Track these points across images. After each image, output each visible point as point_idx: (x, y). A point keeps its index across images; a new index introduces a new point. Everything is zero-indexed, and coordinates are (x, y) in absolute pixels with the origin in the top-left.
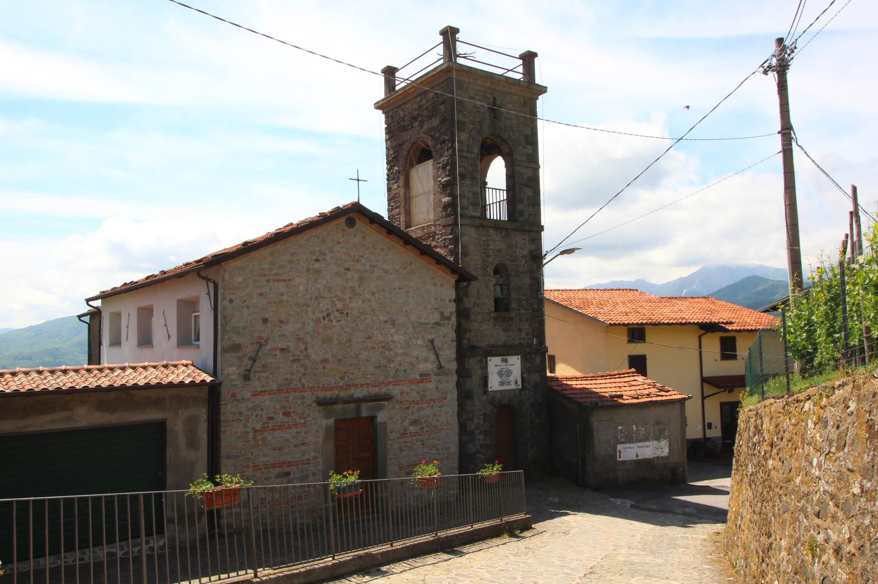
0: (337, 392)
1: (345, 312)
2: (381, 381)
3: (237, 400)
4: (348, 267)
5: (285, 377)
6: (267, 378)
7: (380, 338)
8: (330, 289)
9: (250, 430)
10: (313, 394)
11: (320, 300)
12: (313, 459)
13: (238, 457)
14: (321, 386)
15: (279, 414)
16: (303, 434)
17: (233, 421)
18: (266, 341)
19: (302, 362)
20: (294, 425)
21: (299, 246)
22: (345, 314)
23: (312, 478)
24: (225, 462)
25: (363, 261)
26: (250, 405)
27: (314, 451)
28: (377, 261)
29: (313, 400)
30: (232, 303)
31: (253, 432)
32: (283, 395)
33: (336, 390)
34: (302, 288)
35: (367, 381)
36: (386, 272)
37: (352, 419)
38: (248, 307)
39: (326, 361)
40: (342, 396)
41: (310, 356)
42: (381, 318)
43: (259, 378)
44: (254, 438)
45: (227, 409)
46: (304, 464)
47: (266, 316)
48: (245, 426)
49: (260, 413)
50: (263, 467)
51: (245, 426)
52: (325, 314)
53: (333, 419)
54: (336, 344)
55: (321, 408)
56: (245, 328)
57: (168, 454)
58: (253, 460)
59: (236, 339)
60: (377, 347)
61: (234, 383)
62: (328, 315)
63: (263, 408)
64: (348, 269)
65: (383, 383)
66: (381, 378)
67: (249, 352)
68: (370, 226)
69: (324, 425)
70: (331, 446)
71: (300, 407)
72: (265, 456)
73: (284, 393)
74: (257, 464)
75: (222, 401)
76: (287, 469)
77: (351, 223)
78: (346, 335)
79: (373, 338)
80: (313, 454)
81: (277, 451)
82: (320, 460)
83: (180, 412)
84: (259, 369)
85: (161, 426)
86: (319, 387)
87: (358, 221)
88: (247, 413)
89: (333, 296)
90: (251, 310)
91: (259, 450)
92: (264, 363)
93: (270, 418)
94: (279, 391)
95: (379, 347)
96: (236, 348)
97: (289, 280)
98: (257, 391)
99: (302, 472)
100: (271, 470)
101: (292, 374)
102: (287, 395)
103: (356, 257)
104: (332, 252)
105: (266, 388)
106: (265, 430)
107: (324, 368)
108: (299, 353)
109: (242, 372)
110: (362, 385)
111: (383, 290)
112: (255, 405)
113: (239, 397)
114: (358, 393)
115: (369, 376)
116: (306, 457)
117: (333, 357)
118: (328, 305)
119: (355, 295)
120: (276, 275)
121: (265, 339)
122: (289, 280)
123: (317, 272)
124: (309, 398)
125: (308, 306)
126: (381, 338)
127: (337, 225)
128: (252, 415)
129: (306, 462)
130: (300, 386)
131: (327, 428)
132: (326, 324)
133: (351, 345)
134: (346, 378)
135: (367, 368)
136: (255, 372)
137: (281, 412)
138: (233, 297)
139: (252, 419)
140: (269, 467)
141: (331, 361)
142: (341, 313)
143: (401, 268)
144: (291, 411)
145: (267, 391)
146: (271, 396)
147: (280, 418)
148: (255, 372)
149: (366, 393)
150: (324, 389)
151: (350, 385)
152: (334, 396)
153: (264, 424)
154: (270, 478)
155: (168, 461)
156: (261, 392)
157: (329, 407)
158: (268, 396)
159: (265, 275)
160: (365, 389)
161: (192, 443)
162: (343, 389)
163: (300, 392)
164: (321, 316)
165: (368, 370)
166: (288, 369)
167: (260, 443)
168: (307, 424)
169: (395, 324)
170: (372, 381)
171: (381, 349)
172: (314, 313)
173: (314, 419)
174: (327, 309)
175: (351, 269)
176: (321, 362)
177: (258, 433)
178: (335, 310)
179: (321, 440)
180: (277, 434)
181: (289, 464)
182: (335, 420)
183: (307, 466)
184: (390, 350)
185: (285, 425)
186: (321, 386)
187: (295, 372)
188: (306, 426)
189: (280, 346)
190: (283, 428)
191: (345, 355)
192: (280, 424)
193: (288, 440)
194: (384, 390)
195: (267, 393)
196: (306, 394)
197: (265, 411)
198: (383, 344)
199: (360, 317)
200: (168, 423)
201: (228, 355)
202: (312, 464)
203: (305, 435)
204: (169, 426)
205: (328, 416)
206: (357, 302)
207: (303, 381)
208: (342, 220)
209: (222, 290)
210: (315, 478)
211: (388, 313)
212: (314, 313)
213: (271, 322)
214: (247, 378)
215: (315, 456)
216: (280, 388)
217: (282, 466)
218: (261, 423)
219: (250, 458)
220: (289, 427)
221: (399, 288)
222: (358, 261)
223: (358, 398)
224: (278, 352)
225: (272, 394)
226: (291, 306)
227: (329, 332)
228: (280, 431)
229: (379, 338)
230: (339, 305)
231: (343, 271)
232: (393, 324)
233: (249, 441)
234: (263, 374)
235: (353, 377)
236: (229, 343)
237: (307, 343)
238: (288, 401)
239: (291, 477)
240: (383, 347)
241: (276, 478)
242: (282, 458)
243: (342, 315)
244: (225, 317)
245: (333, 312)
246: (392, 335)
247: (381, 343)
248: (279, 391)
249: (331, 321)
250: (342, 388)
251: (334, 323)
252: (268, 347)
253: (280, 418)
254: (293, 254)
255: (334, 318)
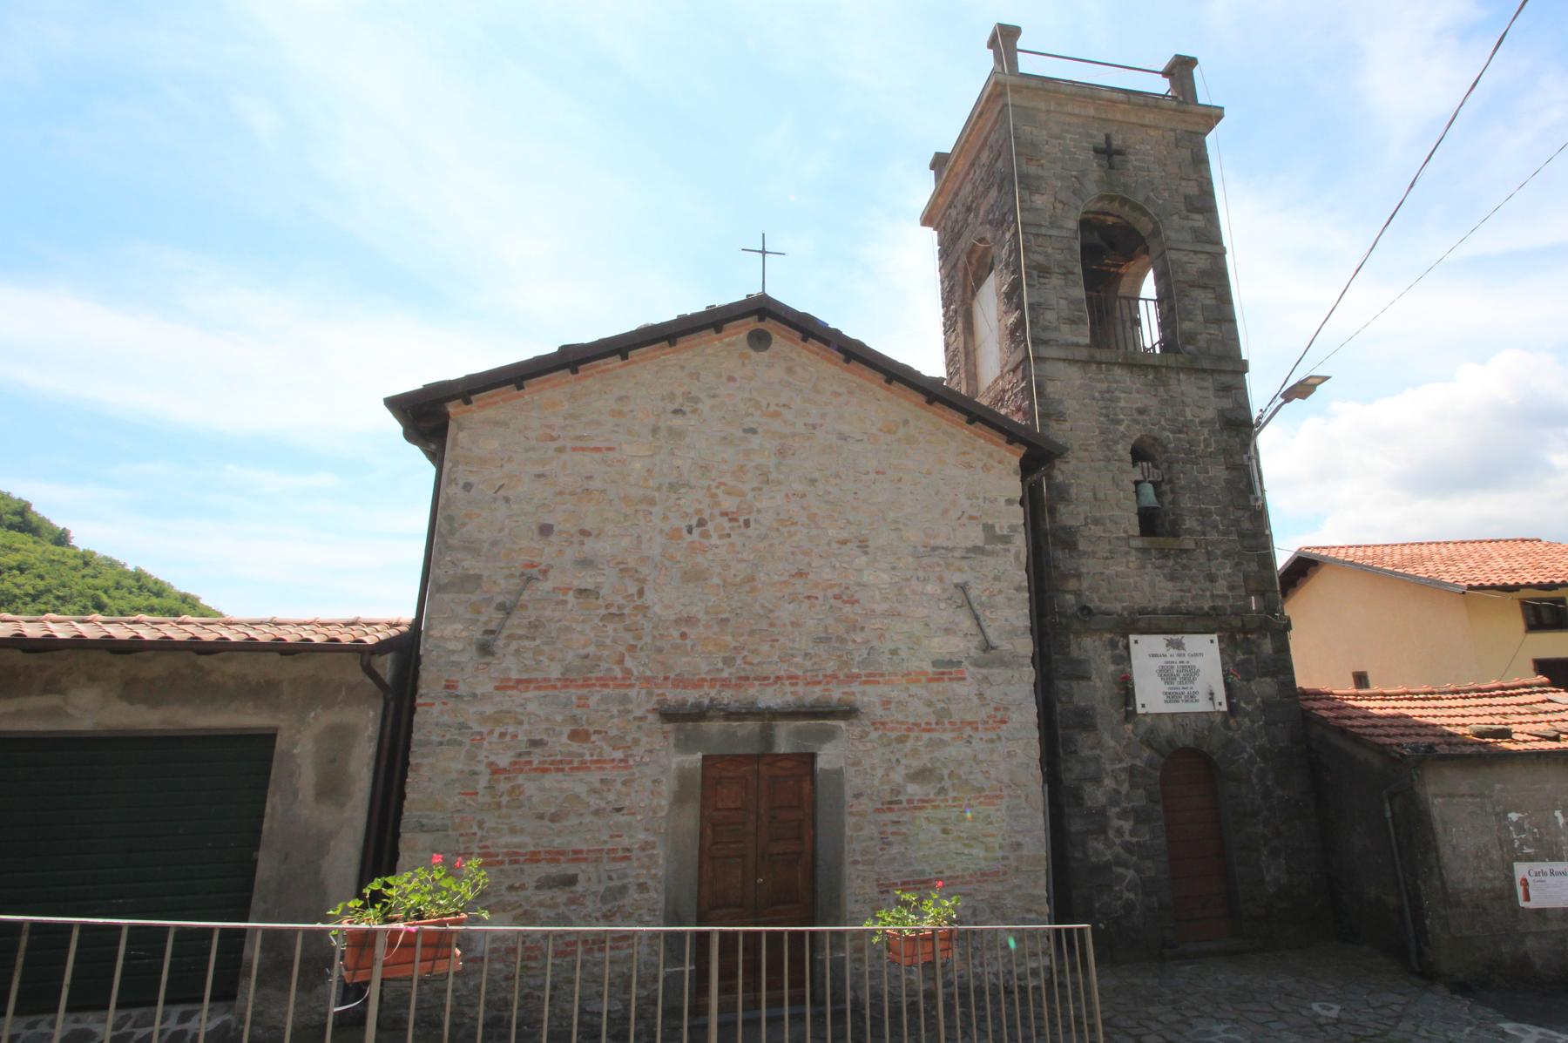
0: (713, 693)
1: (742, 519)
2: (829, 672)
3: (457, 696)
4: (752, 426)
5: (583, 652)
6: (537, 652)
7: (827, 574)
8: (705, 468)
9: (481, 768)
10: (650, 694)
11: (682, 491)
12: (643, 849)
13: (444, 829)
14: (672, 675)
15: (561, 733)
16: (619, 786)
17: (441, 744)
18: (545, 572)
19: (628, 622)
20: (598, 761)
21: (637, 383)
22: (741, 523)
23: (636, 896)
24: (409, 840)
25: (788, 415)
26: (489, 710)
27: (647, 830)
28: (823, 415)
29: (650, 706)
30: (469, 491)
31: (489, 771)
32: (573, 691)
33: (712, 686)
34: (637, 465)
35: (792, 669)
36: (844, 438)
37: (756, 758)
38: (507, 500)
39: (690, 621)
40: (726, 701)
41: (648, 608)
42: (831, 532)
43: (517, 652)
44: (490, 787)
45: (430, 717)
46: (614, 860)
47: (548, 520)
48: (472, 757)
49: (511, 729)
50: (507, 859)
51: (472, 757)
52: (694, 522)
53: (699, 755)
54: (718, 585)
55: (669, 727)
56: (494, 543)
57: (268, 810)
58: (481, 841)
59: (471, 564)
60: (820, 594)
61: (454, 658)
62: (701, 523)
63: (521, 717)
64: (753, 431)
65: (835, 677)
66: (831, 667)
67: (499, 593)
68: (804, 348)
69: (674, 766)
70: (690, 819)
71: (616, 720)
72: (513, 831)
73: (577, 687)
74: (491, 850)
75: (421, 696)
76: (570, 869)
77: (759, 340)
78: (743, 565)
79: (811, 576)
80: (642, 836)
81: (547, 823)
82: (659, 851)
83: (312, 714)
84: (520, 632)
85: (261, 744)
86: (666, 678)
87: (776, 338)
88: (476, 728)
89: (714, 484)
90: (514, 507)
91: (499, 817)
92: (532, 619)
93: (535, 743)
94: (566, 681)
95: (825, 596)
96: (469, 582)
97: (609, 449)
98: (509, 680)
99: (610, 878)
100: (527, 867)
101: (601, 645)
102: (585, 691)
103: (772, 408)
104: (714, 396)
105: (534, 675)
106: (521, 771)
107: (683, 636)
108: (622, 601)
109: (478, 634)
110: (778, 678)
111: (837, 476)
112: (502, 711)
113: (463, 689)
114: (770, 698)
115: (798, 660)
116: (626, 841)
117: (707, 613)
118: (700, 503)
119: (767, 482)
120: (578, 438)
121: (543, 567)
122: (609, 449)
123: (676, 434)
124: (641, 701)
125: (652, 502)
126: (830, 577)
127: (729, 344)
128: (491, 732)
129: (620, 854)
130: (618, 673)
131: (683, 777)
132: (693, 542)
133: (753, 590)
134: (739, 661)
135: (794, 641)
136: (511, 637)
137: (567, 730)
138: (472, 479)
139: (490, 743)
140: (522, 858)
141: (703, 622)
142: (731, 520)
143: (881, 430)
144: (591, 730)
145: (536, 680)
146: (542, 693)
147: (561, 743)
148: (511, 637)
149: (790, 698)
150: (680, 682)
151: (747, 678)
152: (706, 701)
153: (520, 755)
154: (523, 887)
155: (266, 826)
156: (519, 681)
157: (690, 725)
158: (537, 693)
159: (553, 439)
160: (788, 689)
161: (331, 788)
162: (727, 686)
163: (618, 686)
164: (683, 525)
165: (796, 645)
166: (592, 635)
167: (505, 799)
168: (631, 762)
169: (867, 546)
170: (806, 671)
171: (833, 602)
172: (665, 518)
173: (651, 751)
174: (699, 511)
175: (760, 430)
176: (677, 622)
177: (502, 777)
178: (716, 512)
179: (664, 803)
180: (549, 780)
181: (577, 856)
182: (704, 757)
183: (624, 865)
184: (853, 602)
185: (570, 762)
186: (672, 675)
187: (608, 642)
188: (626, 768)
189: (577, 583)
190: (567, 767)
191: (739, 611)
192: (559, 758)
193: (577, 797)
194: (836, 694)
195: (532, 686)
196: (633, 693)
197: (526, 727)
198: (836, 591)
199: (778, 530)
200: (278, 738)
201: (447, 597)
202: (638, 859)
203: (624, 789)
204: (281, 744)
205: (684, 745)
206: (772, 498)
207: (629, 663)
208: (742, 336)
209: (451, 464)
210: (646, 896)
211: (849, 522)
212: (665, 518)
213: (561, 532)
214: (485, 649)
215: (647, 843)
216: (567, 677)
217: (557, 861)
218: (513, 753)
219: (475, 834)
220: (584, 766)
221: (877, 473)
222: (776, 415)
223: (768, 708)
224: (571, 597)
225: (546, 688)
226: (611, 501)
227: (700, 559)
228: (560, 776)
229: (825, 577)
230: (729, 504)
231: (739, 433)
232: (863, 546)
233: (476, 794)
234: (527, 643)
235: (756, 660)
236: (451, 572)
237: (643, 581)
238: (586, 706)
239: (579, 888)
240: (836, 597)
241: (538, 888)
242: (557, 841)
243: (736, 524)
244: (450, 519)
245: (712, 517)
246: (860, 570)
247: (832, 586)
248: (566, 681)
249: (705, 535)
250: (725, 683)
251: (715, 540)
252: (545, 586)
253: (561, 743)
254: (621, 399)
255: (715, 531)
